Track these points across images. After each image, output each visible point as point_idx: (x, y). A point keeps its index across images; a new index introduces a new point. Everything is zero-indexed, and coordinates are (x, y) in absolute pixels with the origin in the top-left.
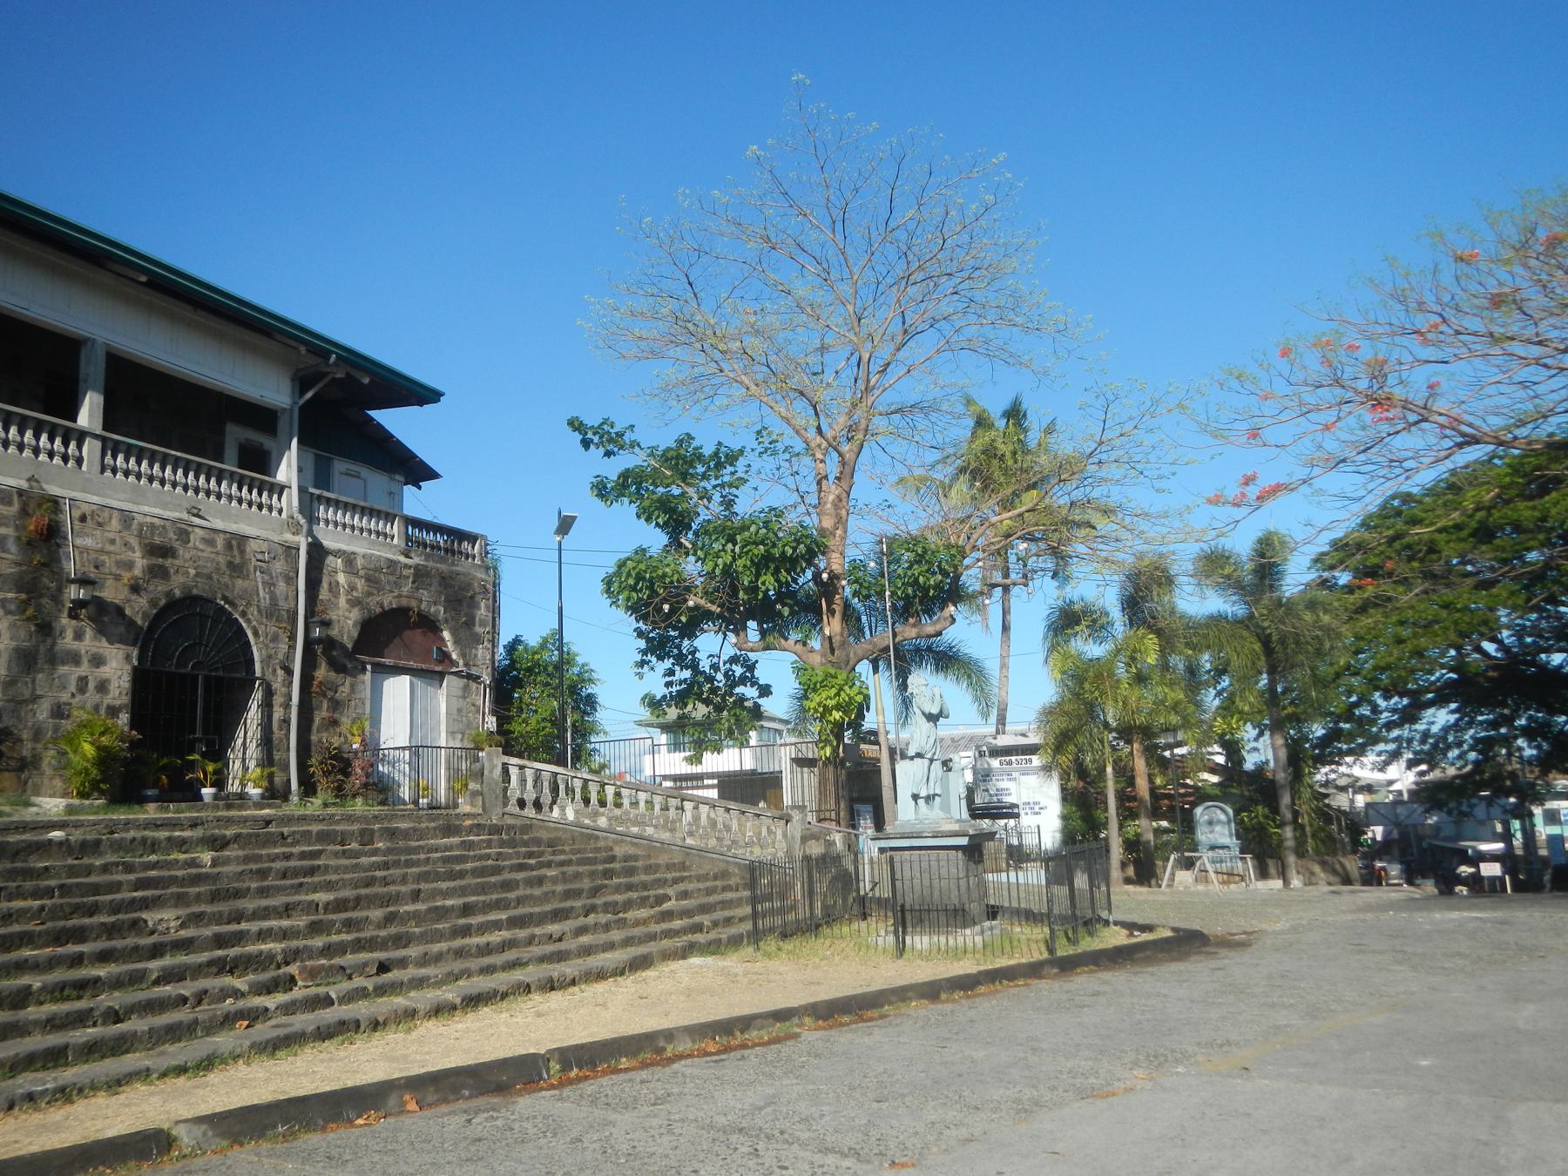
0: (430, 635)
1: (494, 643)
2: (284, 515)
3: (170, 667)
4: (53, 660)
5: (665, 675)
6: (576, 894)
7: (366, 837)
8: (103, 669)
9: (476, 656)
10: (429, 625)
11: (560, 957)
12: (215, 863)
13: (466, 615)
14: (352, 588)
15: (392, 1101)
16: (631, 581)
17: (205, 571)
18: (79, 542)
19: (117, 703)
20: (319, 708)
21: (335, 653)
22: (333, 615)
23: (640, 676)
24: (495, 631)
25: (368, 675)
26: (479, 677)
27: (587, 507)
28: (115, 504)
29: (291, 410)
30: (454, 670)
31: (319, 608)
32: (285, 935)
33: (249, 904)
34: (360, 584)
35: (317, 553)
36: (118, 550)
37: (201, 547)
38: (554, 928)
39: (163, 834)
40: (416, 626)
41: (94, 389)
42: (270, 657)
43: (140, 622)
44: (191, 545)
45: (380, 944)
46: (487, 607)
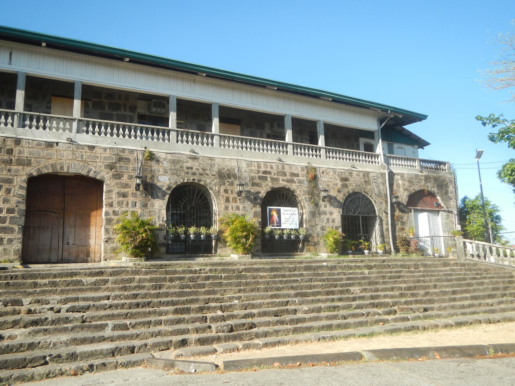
0: (433, 198)
1: (456, 199)
2: (380, 164)
3: (351, 214)
4: (320, 214)
6: (498, 289)
7: (416, 266)
8: (333, 216)
9: (450, 204)
11: (493, 312)
12: (369, 273)
13: (445, 190)
14: (404, 185)
15: (431, 354)
16: (509, 172)
17: (358, 184)
18: (322, 179)
19: (338, 225)
20: (398, 224)
21: (401, 207)
22: (398, 194)
25: (413, 213)
27: (488, 146)
28: (331, 167)
29: (378, 130)
30: (443, 209)
31: (394, 192)
32: (392, 297)
33: (380, 287)
34: (407, 183)
35: (391, 175)
36: (333, 181)
37: (356, 177)
38: (489, 301)
39: (353, 264)
40: (427, 195)
42: (380, 209)
43: (341, 201)
44: (353, 177)
45: (425, 302)
46: (453, 187)
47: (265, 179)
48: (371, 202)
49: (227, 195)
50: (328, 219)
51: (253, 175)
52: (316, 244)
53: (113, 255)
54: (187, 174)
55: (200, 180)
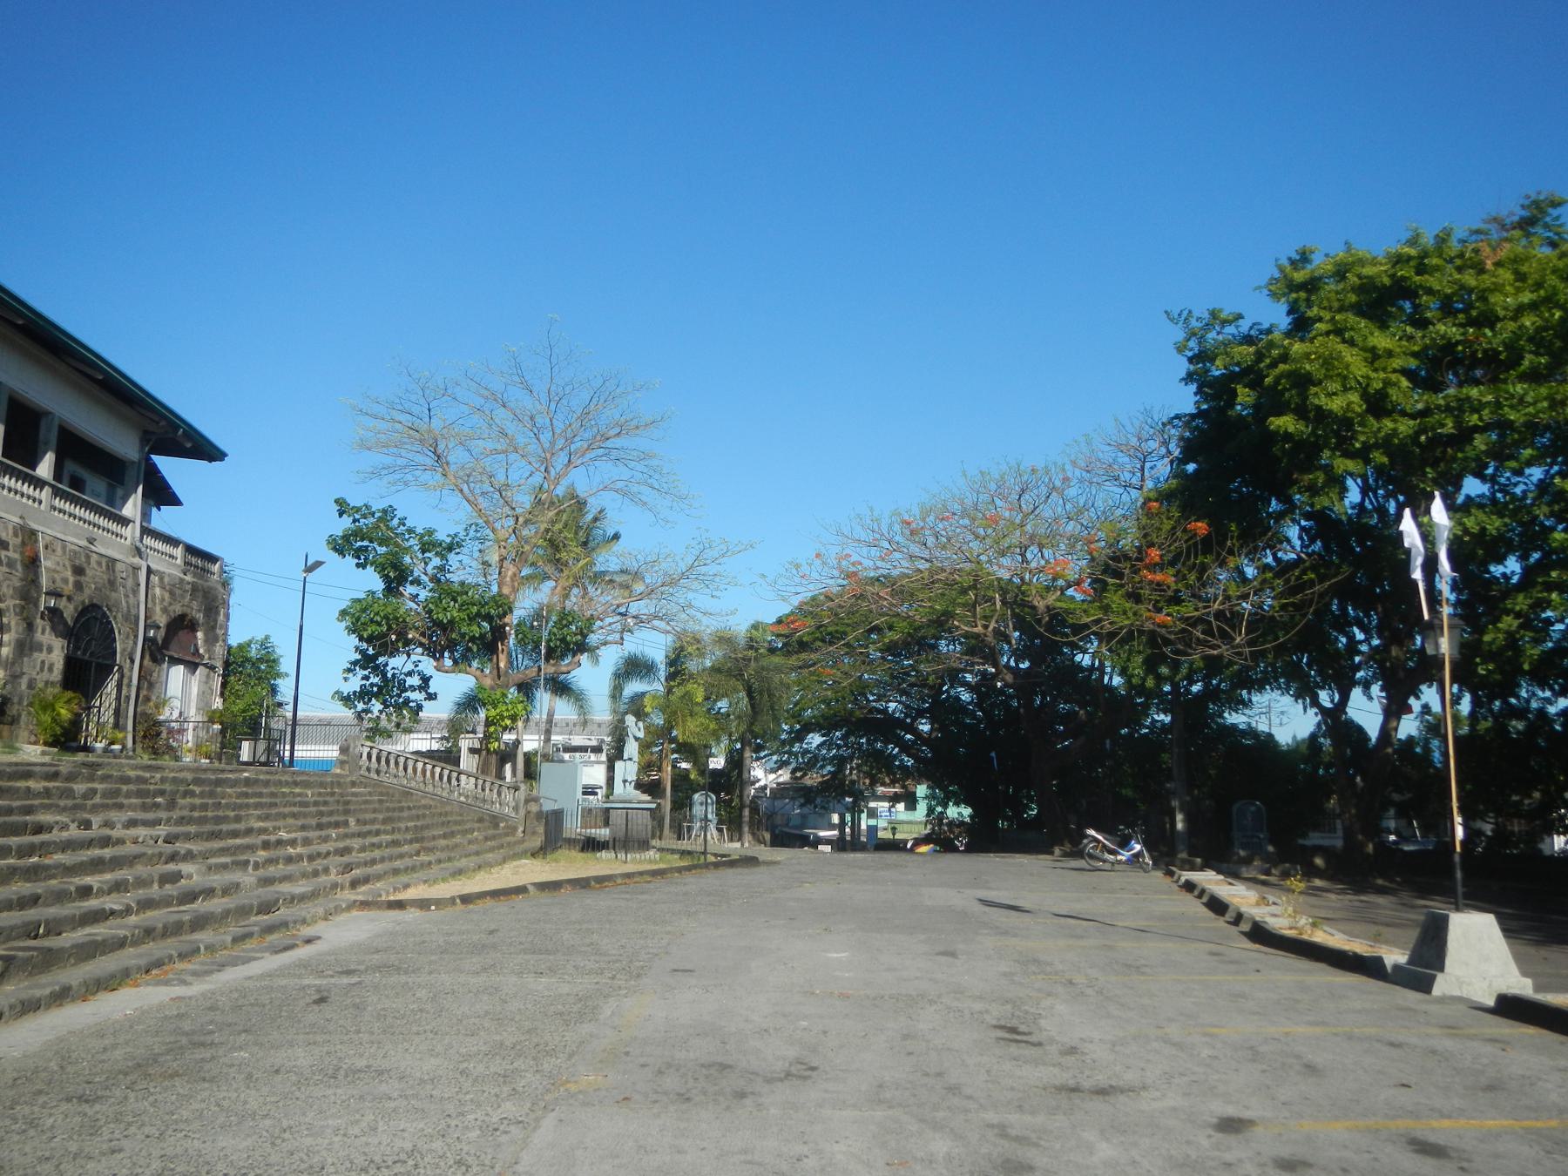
5: (363, 679)
10: (193, 627)
14: (163, 600)
17: (99, 586)
23: (346, 679)
24: (226, 634)
26: (215, 667)
28: (59, 536)
34: (167, 596)
35: (149, 571)
40: (187, 627)
41: (51, 450)
48: (112, 631)
50: (43, 662)
52: (14, 721)
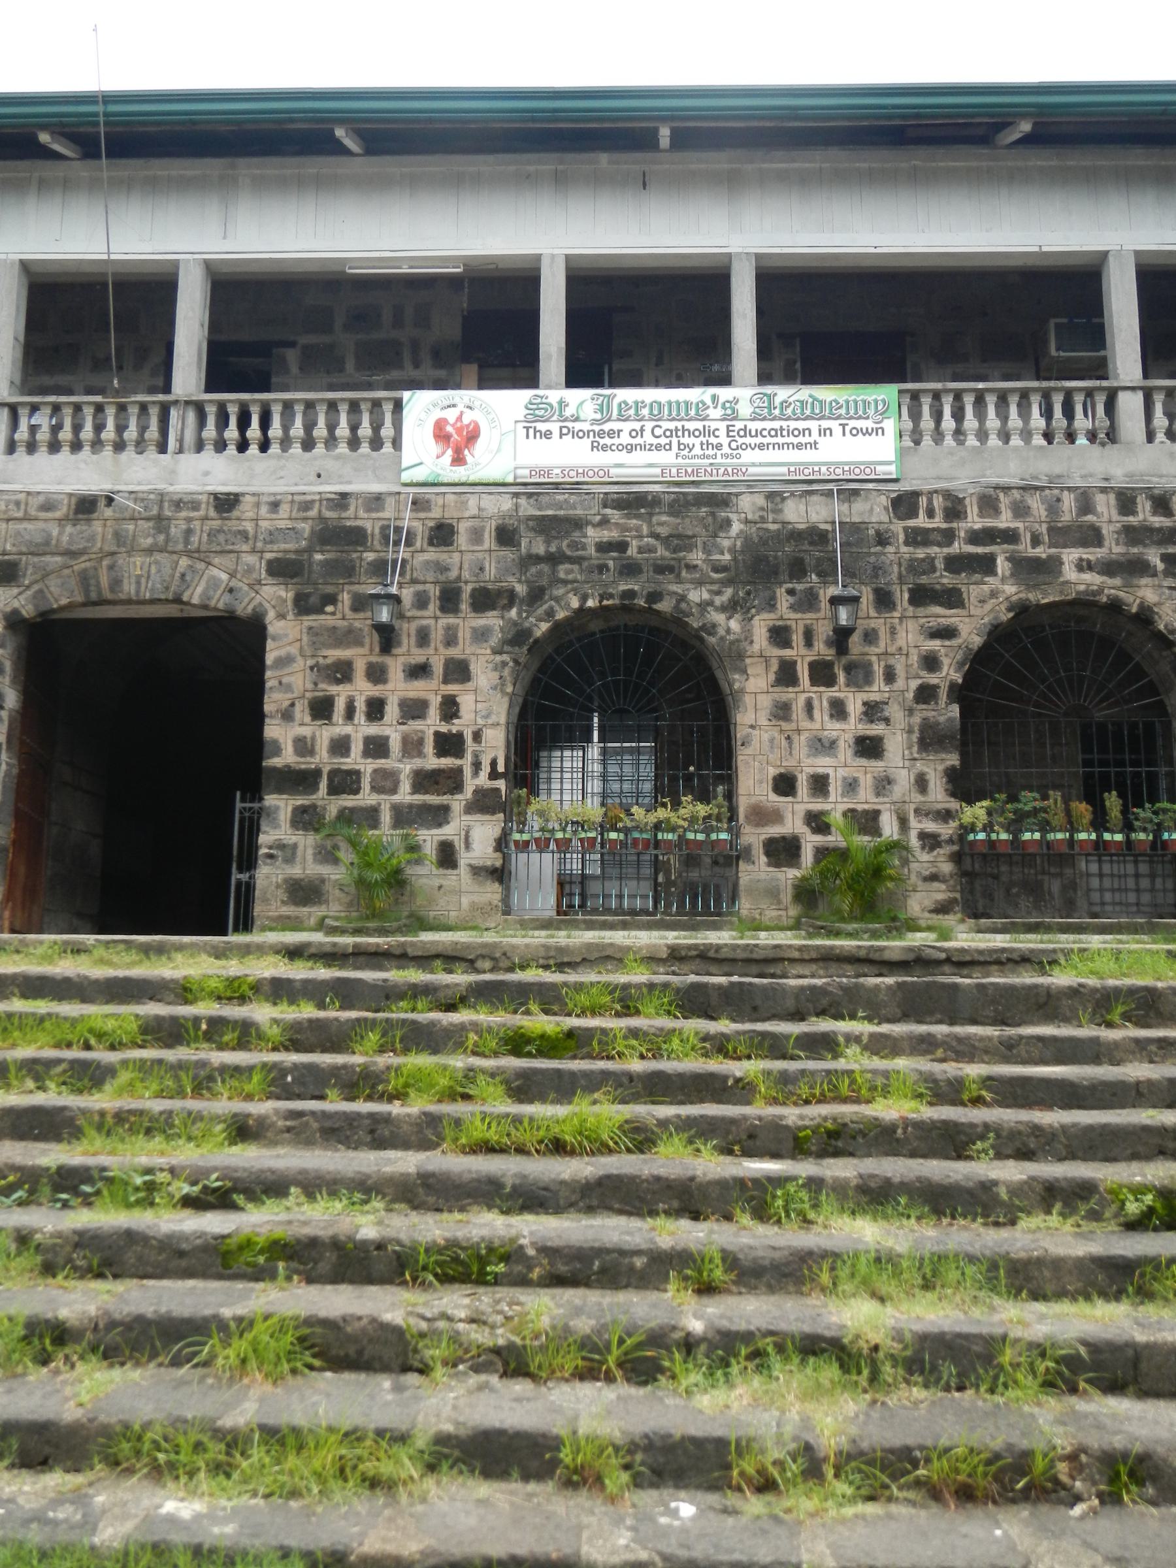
47: (986, 565)
49: (787, 653)
51: (921, 553)
53: (289, 910)
54: (601, 572)
55: (655, 597)
